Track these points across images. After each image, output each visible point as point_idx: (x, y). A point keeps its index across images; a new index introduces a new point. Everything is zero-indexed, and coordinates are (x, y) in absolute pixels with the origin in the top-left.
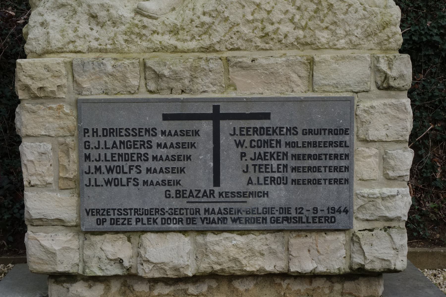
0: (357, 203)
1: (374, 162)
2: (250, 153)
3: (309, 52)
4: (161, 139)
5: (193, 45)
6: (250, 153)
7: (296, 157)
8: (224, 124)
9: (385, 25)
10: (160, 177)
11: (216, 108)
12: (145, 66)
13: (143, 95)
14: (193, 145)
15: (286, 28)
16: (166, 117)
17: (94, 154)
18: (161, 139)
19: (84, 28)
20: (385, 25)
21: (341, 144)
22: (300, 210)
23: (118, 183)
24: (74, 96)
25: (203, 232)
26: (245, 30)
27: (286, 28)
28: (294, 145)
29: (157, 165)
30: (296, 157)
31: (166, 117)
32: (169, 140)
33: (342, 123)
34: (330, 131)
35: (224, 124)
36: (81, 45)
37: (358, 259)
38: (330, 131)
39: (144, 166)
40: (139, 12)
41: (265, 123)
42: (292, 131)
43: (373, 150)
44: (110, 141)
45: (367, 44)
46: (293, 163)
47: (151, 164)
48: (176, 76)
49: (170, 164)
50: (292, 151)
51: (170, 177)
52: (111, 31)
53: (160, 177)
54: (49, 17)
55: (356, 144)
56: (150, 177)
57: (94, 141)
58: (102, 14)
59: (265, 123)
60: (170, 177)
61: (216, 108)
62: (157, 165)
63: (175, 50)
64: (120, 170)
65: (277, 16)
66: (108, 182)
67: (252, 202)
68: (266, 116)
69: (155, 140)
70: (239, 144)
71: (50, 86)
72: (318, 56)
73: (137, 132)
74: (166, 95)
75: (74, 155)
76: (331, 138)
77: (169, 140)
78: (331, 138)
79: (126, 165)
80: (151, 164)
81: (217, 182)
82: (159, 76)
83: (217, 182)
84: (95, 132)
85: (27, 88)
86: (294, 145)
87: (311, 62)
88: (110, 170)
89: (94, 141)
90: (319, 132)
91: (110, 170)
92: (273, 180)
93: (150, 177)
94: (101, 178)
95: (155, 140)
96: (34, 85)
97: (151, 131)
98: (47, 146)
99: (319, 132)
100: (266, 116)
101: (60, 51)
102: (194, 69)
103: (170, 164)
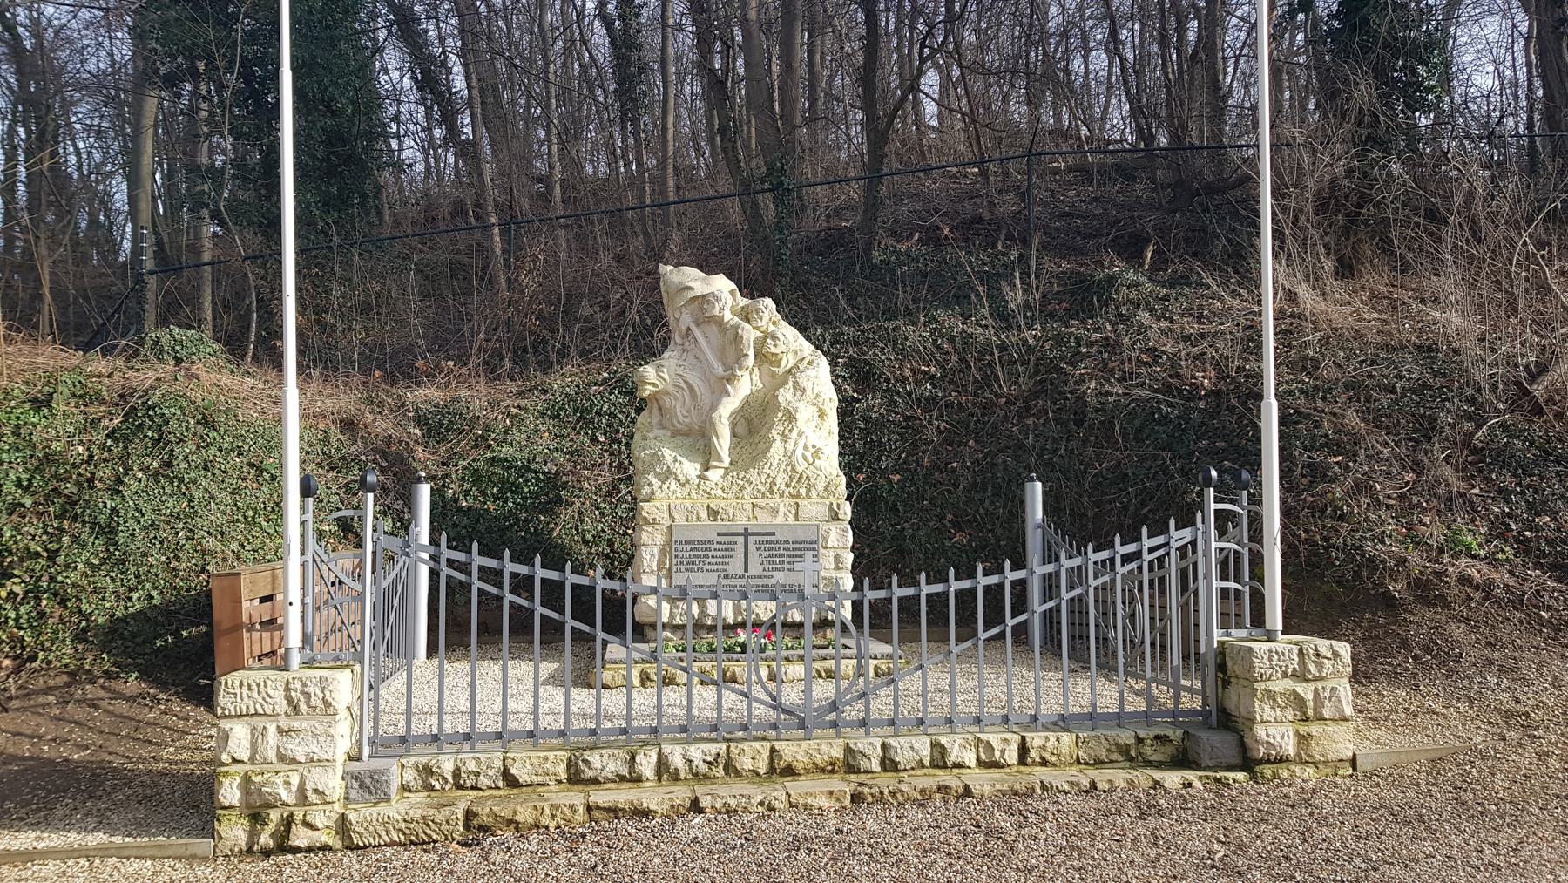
2: (764, 554)
6: (764, 554)
7: (788, 556)
8: (751, 539)
10: (716, 567)
11: (746, 530)
12: (708, 507)
14: (733, 550)
16: (719, 534)
22: (791, 586)
23: (692, 570)
28: (788, 549)
29: (714, 560)
30: (788, 556)
31: (719, 534)
32: (720, 547)
35: (751, 539)
39: (707, 561)
41: (772, 538)
42: (787, 542)
44: (689, 547)
47: (710, 560)
49: (721, 560)
50: (786, 553)
51: (720, 567)
53: (716, 567)
56: (709, 567)
59: (772, 538)
60: (720, 567)
61: (746, 530)
62: (714, 560)
64: (694, 563)
66: (687, 570)
67: (766, 581)
68: (774, 534)
69: (713, 547)
70: (758, 549)
73: (704, 542)
76: (808, 546)
77: (720, 547)
78: (808, 546)
79: (697, 560)
80: (710, 560)
81: (746, 570)
83: (746, 570)
84: (681, 543)
85: (645, 518)
86: (788, 549)
87: (797, 504)
88: (688, 563)
90: (801, 543)
91: (688, 563)
92: (777, 569)
93: (709, 567)
94: (683, 568)
95: (713, 547)
99: (801, 543)
100: (774, 534)
103: (721, 560)
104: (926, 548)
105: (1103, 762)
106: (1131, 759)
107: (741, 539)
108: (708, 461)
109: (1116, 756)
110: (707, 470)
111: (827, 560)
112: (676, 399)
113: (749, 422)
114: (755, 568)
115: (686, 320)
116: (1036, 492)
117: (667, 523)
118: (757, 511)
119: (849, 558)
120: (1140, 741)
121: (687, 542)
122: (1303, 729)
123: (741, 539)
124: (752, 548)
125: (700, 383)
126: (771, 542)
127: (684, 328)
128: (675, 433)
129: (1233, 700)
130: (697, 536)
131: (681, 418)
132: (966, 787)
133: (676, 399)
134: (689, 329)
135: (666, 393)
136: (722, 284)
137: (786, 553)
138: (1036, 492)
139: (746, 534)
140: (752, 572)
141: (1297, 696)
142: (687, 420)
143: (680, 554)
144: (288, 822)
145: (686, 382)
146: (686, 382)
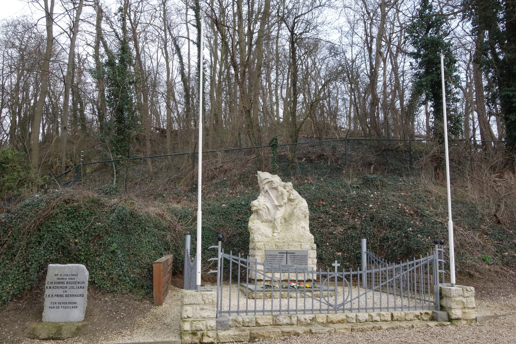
0: (309, 268)
1: (311, 261)
2: (292, 259)
3: (300, 243)
4: (278, 256)
5: (281, 241)
6: (292, 259)
9: (312, 239)
15: (296, 239)
16: (279, 253)
17: (268, 259)
18: (278, 256)
19: (264, 238)
20: (312, 239)
21: (306, 258)
24: (264, 249)
25: (284, 272)
26: (290, 239)
27: (296, 239)
29: (277, 261)
31: (279, 253)
33: (306, 255)
34: (304, 256)
36: (264, 241)
37: (309, 278)
38: (304, 256)
40: (273, 235)
41: (294, 254)
43: (311, 259)
44: (270, 257)
45: (310, 242)
46: (299, 261)
48: (281, 246)
52: (269, 239)
54: (258, 236)
55: (309, 259)
57: (267, 257)
58: (267, 236)
59: (294, 254)
62: (277, 261)
63: (279, 242)
64: (272, 261)
65: (295, 237)
68: (294, 253)
71: (261, 247)
72: (302, 244)
73: (274, 255)
75: (264, 259)
82: (278, 246)
85: (257, 248)
87: (301, 245)
89: (267, 257)
94: (268, 263)
96: (259, 247)
97: (277, 255)
98: (260, 257)
100: (294, 253)
101: (261, 242)
102: (283, 245)
104: (329, 258)
105: (412, 320)
106: (419, 319)
107: (285, 255)
108: (274, 230)
109: (415, 318)
110: (273, 233)
111: (310, 261)
112: (263, 211)
113: (285, 219)
114: (289, 263)
115: (267, 187)
116: (364, 241)
117: (264, 249)
118: (290, 247)
119: (316, 261)
120: (421, 314)
121: (270, 255)
122: (464, 311)
123: (285, 255)
124: (288, 257)
125: (270, 207)
126: (294, 256)
127: (265, 190)
128: (263, 221)
129: (444, 302)
130: (272, 253)
131: (264, 217)
132: (381, 327)
133: (263, 211)
134: (267, 191)
135: (260, 210)
136: (276, 179)
138: (364, 241)
139: (287, 253)
140: (288, 265)
141: (462, 301)
142: (266, 218)
144: (203, 335)
145: (266, 206)
146: (266, 206)
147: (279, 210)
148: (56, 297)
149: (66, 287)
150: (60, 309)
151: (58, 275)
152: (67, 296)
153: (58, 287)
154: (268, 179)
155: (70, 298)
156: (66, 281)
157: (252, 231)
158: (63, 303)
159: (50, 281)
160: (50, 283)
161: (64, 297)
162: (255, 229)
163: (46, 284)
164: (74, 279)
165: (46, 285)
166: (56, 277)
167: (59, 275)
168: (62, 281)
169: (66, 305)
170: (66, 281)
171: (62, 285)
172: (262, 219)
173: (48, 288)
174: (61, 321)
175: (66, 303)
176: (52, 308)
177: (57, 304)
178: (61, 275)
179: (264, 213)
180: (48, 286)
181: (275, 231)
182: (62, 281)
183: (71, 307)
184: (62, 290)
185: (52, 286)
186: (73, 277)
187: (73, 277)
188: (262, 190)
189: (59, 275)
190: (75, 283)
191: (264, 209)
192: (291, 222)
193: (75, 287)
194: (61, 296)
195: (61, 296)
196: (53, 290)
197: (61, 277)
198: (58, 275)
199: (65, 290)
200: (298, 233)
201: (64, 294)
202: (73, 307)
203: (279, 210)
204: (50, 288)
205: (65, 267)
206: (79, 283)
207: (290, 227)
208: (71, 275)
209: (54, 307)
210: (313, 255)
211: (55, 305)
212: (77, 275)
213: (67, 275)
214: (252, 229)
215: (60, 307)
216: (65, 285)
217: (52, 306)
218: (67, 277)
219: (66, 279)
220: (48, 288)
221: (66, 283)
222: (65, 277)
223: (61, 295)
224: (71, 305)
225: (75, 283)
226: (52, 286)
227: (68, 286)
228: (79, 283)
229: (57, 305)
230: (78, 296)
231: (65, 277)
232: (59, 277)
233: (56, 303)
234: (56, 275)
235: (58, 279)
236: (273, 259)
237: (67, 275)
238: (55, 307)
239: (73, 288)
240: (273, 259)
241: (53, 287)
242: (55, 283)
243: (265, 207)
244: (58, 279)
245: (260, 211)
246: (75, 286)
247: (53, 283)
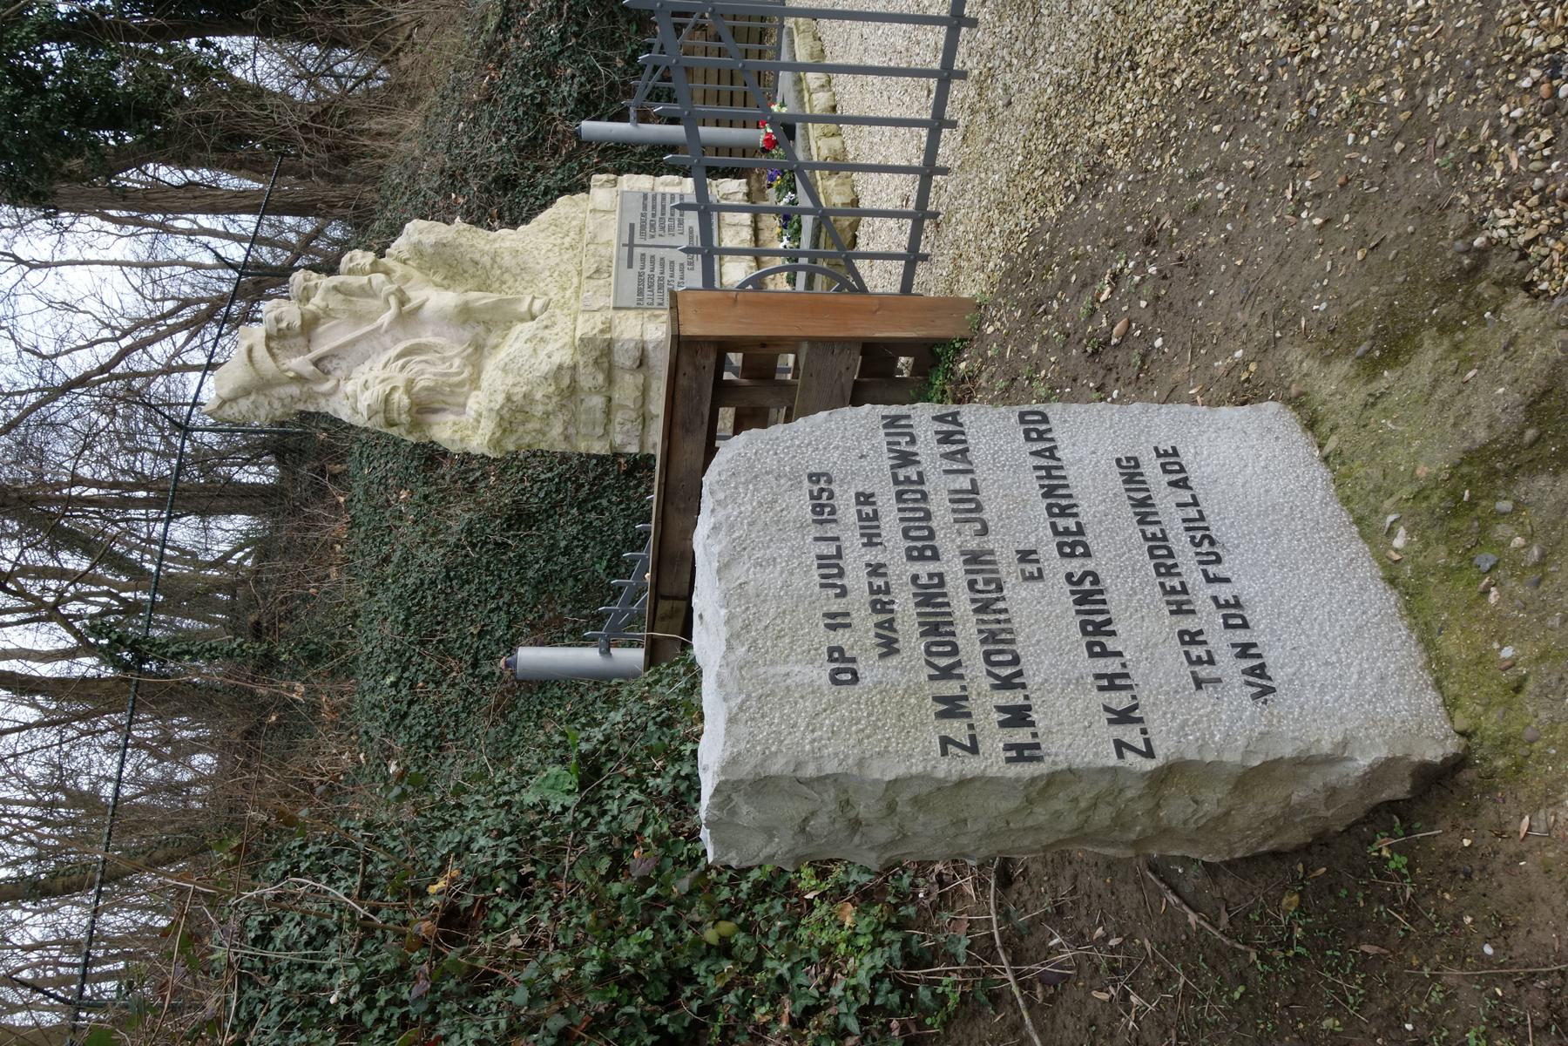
13: (612, 279)
16: (630, 266)
18: (647, 271)
21: (654, 197)
31: (630, 266)
35: (637, 241)
50: (659, 215)
68: (632, 226)
74: (613, 270)
82: (597, 271)
85: (602, 331)
96: (600, 326)
107: (637, 251)
112: (422, 372)
115: (299, 363)
117: (610, 313)
121: (640, 292)
126: (643, 227)
133: (422, 372)
135: (410, 384)
137: (659, 215)
139: (631, 245)
142: (457, 362)
143: (656, 301)
147: (420, 307)
148: (1111, 644)
149: (974, 559)
150: (1244, 586)
151: (836, 654)
152: (1073, 543)
153: (990, 637)
154: (250, 350)
155: (1086, 512)
156: (901, 571)
157: (518, 398)
158: (1166, 568)
159: (934, 730)
160: (957, 729)
161: (1090, 565)
162: (510, 380)
163: (972, 766)
164: (865, 498)
165: (992, 760)
166: (871, 669)
167: (841, 638)
168: (905, 604)
169: (1180, 541)
170: (901, 571)
171: (961, 603)
172: (461, 384)
173: (1022, 736)
174: (1367, 570)
175: (1158, 546)
176: (1259, 671)
177: (1190, 624)
178: (836, 621)
179: (432, 369)
180: (995, 741)
181: (524, 307)
182: (905, 604)
183: (1186, 497)
184: (1019, 596)
185: (986, 703)
186: (848, 511)
187: (848, 511)
188: (312, 396)
189: (841, 638)
190: (911, 493)
191: (411, 366)
192: (486, 260)
193: (963, 482)
194: (1088, 594)
195: (1088, 594)
196: (1033, 677)
197: (865, 621)
198: (836, 654)
199: (1009, 569)
200: (542, 235)
201: (1056, 566)
202: (1183, 484)
203: (420, 307)
204: (1018, 716)
205: (735, 595)
206: (906, 459)
207: (507, 260)
208: (831, 531)
209: (1245, 650)
210: (643, 182)
211: (1220, 641)
212: (814, 477)
213: (832, 567)
214: (509, 399)
215: (1224, 593)
216: (954, 570)
217: (1230, 667)
218: (856, 559)
219: (876, 570)
220: (1022, 736)
221: (923, 569)
222: (857, 579)
223: (1083, 598)
224: (1165, 500)
225: (911, 493)
226: (986, 703)
227: (952, 541)
228: (906, 459)
229: (1208, 620)
230: (1051, 453)
231: (857, 579)
232: (861, 638)
233: (1190, 638)
234: (844, 670)
235: (889, 647)
236: (661, 287)
237: (832, 567)
238: (1242, 636)
239: (968, 503)
240: (661, 287)
241: (1006, 684)
242: (946, 673)
243: (400, 362)
244: (889, 647)
245: (421, 383)
246: (940, 488)
247: (951, 688)
